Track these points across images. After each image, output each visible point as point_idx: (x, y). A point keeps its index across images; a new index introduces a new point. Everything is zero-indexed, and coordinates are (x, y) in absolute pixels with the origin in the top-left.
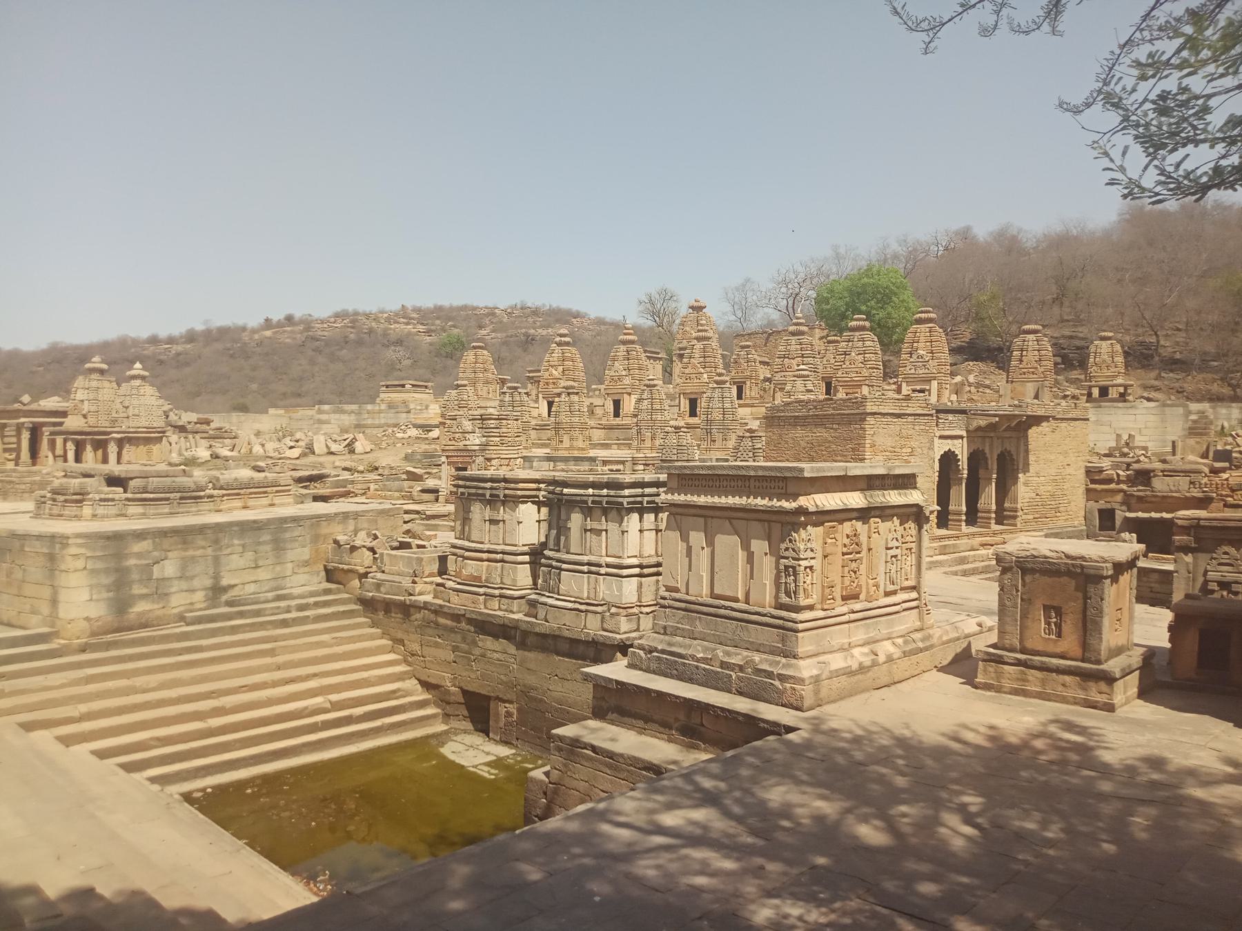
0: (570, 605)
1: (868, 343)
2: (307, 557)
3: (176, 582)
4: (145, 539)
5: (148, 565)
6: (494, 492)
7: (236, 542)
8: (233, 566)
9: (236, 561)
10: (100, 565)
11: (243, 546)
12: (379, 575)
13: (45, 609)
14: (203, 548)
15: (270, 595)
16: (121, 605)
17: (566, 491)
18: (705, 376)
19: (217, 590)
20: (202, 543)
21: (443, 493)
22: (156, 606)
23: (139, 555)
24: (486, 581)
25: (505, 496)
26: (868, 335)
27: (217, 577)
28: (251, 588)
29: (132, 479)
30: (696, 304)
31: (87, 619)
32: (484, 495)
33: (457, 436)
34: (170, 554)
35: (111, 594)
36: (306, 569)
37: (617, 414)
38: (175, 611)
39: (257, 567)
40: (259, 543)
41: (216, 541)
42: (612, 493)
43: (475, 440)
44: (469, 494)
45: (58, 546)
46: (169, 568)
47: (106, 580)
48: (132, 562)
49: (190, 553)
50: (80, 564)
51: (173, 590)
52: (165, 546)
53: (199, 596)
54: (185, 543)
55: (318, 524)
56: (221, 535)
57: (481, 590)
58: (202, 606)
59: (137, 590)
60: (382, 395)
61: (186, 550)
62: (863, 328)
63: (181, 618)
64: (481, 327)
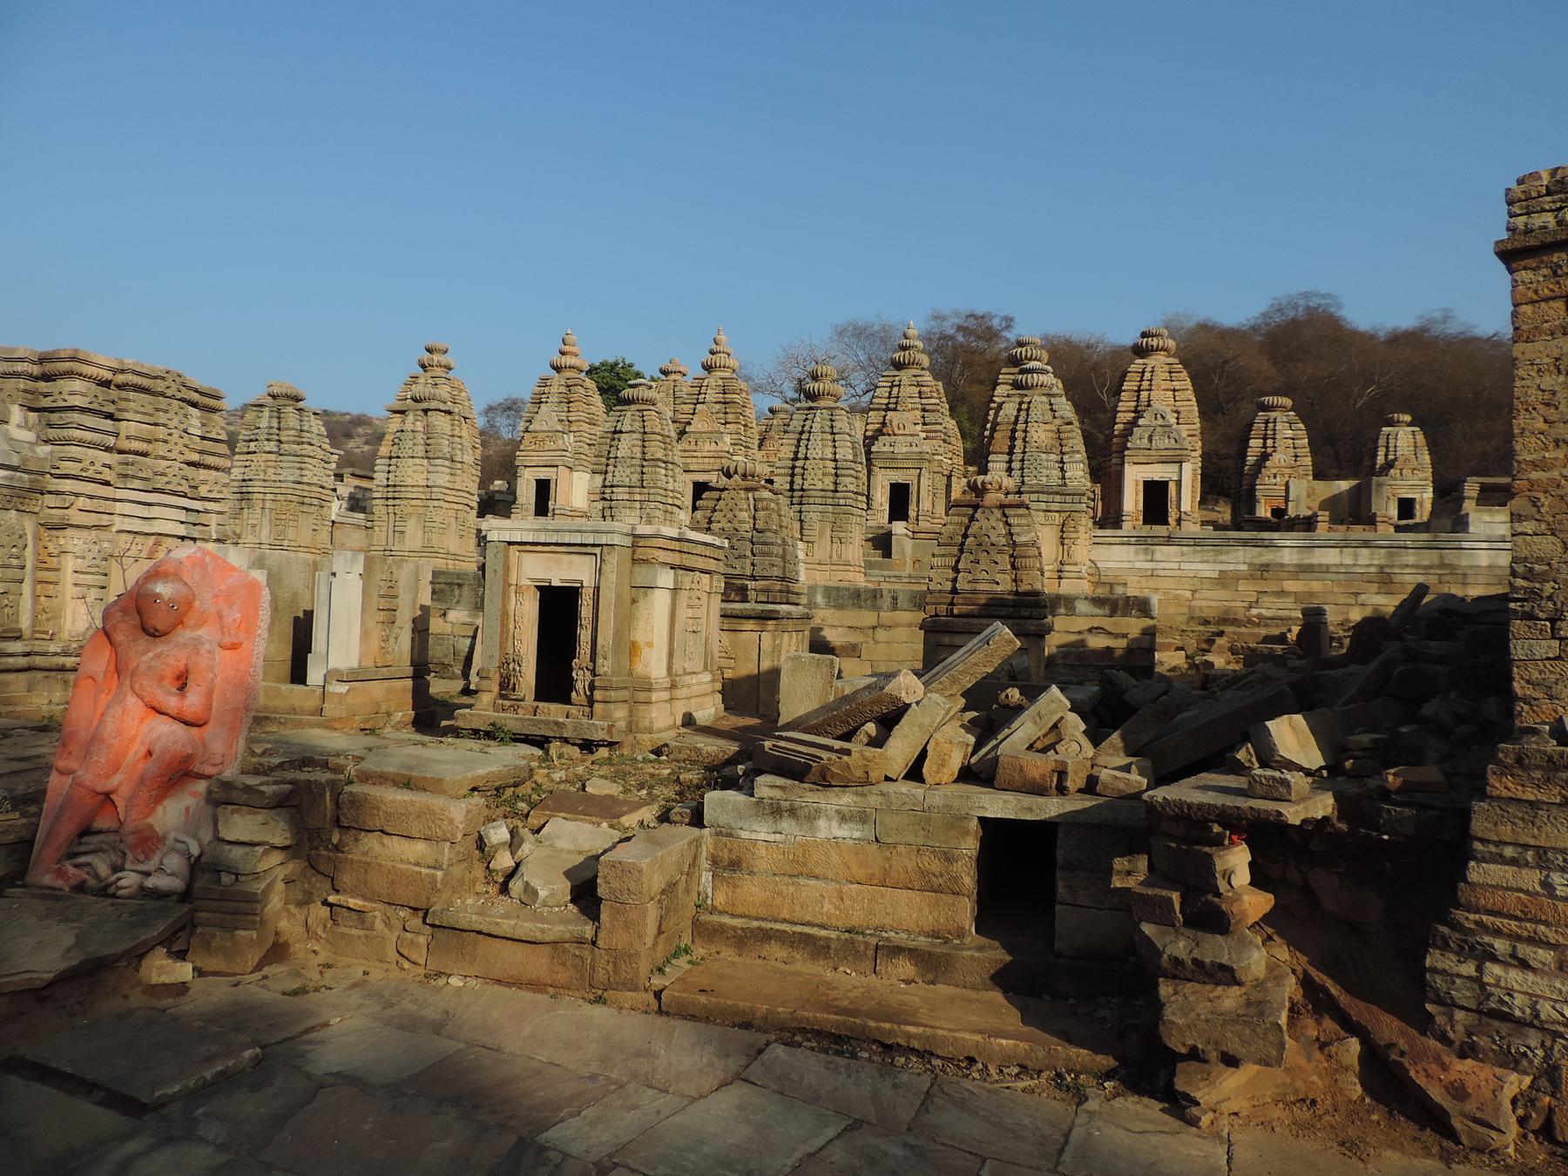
18: (727, 439)
37: (542, 508)
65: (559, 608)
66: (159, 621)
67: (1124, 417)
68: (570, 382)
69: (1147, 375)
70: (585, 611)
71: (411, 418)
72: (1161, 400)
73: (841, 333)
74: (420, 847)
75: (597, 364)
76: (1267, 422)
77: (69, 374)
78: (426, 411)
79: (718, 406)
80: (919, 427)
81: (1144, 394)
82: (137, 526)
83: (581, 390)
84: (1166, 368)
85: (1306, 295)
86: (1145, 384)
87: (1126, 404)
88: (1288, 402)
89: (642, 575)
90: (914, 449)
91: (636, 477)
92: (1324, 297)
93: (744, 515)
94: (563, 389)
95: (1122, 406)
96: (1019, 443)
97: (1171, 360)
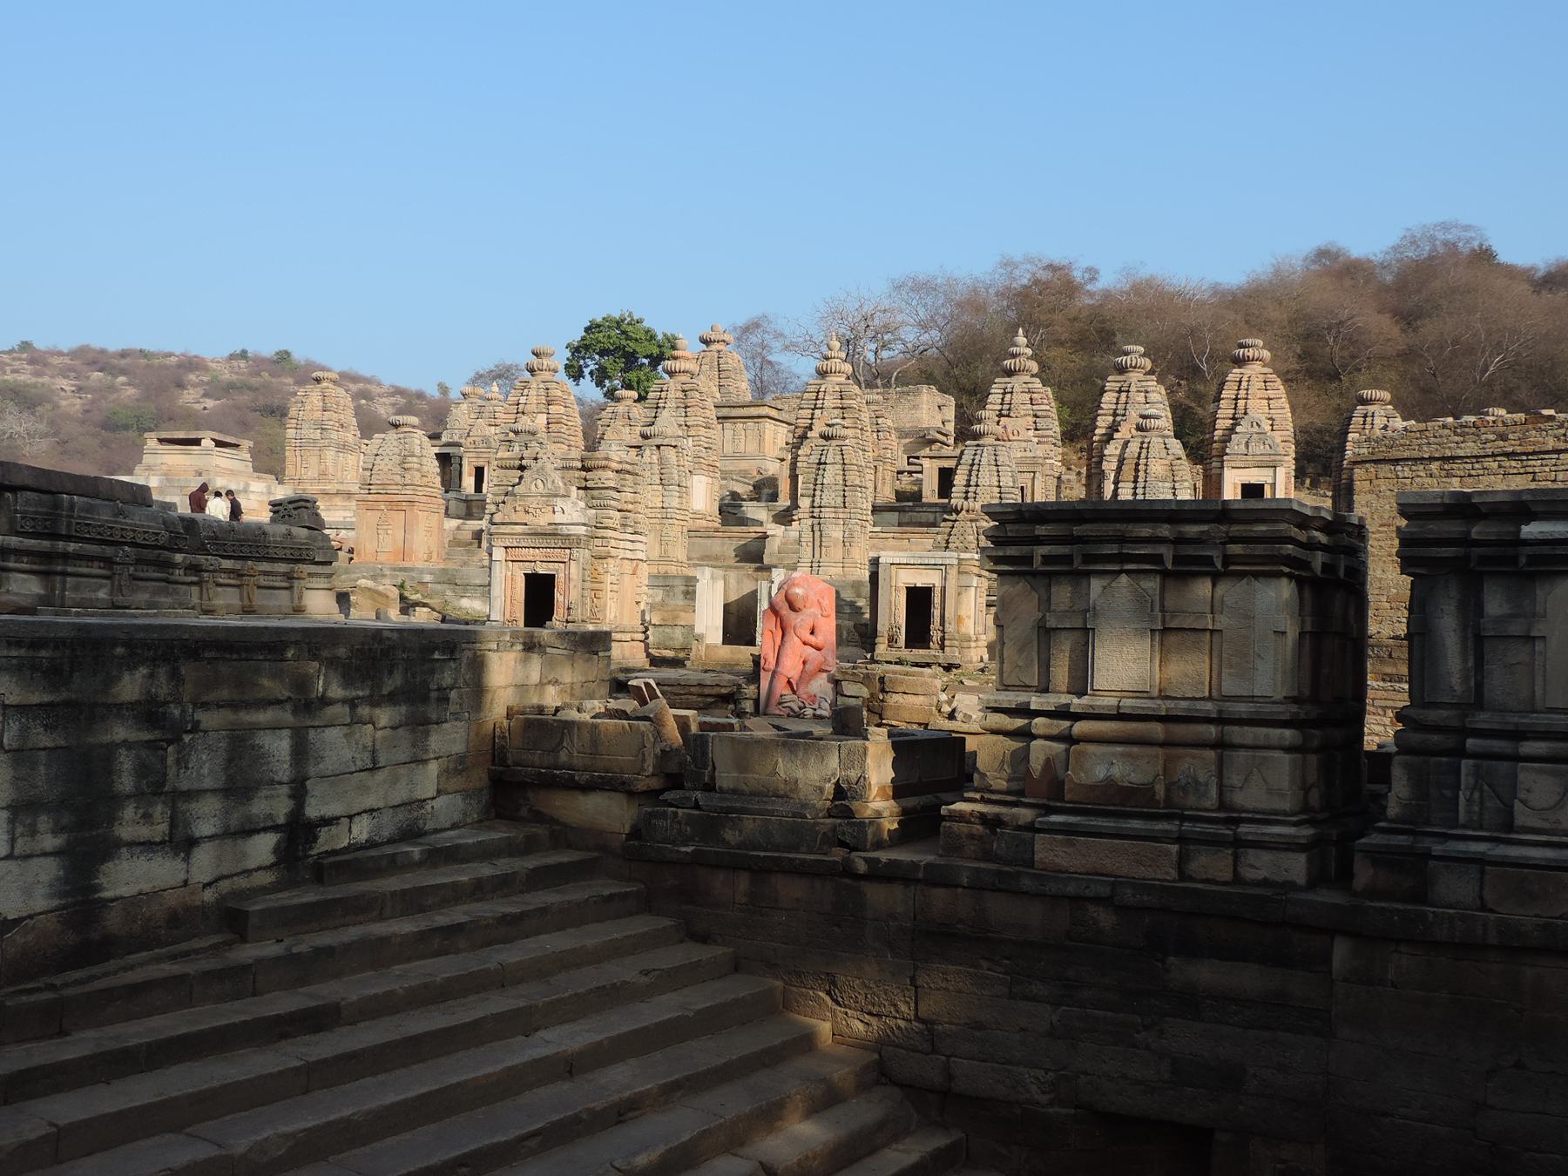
2: (459, 748)
5: (149, 745)
6: (1190, 551)
8: (330, 763)
9: (336, 745)
11: (352, 703)
17: (1531, 530)
24: (1168, 801)
25: (1227, 560)
26: (1152, 383)
27: (299, 791)
28: (361, 830)
39: (374, 768)
43: (571, 512)
53: (263, 848)
58: (266, 878)
59: (129, 825)
60: (147, 459)
64: (181, 385)
65: (919, 600)
66: (798, 605)
67: (1223, 424)
68: (686, 387)
69: (1244, 384)
70: (937, 600)
71: (648, 452)
72: (1257, 409)
73: (898, 288)
74: (921, 698)
75: (599, 320)
76: (1365, 416)
77: (604, 468)
78: (658, 447)
79: (837, 412)
80: (1031, 433)
81: (1241, 403)
82: (629, 555)
83: (697, 395)
84: (1262, 378)
85: (1445, 227)
86: (1242, 393)
87: (1225, 411)
88: (1387, 395)
89: (964, 580)
90: (1029, 454)
91: (839, 500)
92: (1467, 228)
93: (971, 538)
94: (681, 395)
95: (1220, 414)
96: (1141, 474)
97: (1266, 370)
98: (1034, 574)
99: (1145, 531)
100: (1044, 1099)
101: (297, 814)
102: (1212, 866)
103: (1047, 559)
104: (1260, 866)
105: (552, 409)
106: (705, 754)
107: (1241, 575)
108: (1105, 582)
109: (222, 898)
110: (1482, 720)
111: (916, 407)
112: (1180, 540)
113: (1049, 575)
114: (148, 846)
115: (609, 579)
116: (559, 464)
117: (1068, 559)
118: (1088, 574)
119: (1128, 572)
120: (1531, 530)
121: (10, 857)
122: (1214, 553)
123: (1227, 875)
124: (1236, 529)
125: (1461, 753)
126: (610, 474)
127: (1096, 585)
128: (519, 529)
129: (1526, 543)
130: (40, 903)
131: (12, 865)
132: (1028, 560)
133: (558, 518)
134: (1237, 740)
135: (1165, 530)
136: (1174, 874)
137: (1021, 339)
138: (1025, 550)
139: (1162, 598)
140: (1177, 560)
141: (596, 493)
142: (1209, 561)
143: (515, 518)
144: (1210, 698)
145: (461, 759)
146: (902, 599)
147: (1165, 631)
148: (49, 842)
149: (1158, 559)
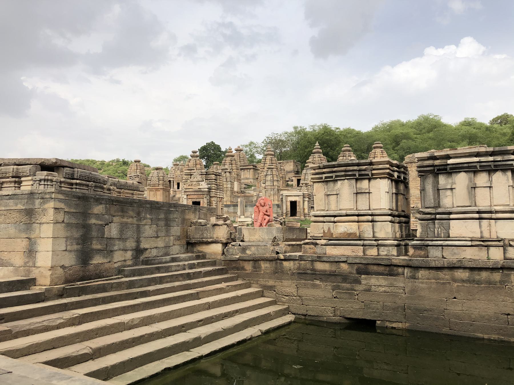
0: (469, 243)
1: (353, 158)
2: (179, 234)
3: (117, 242)
4: (101, 204)
5: (101, 225)
6: (363, 173)
7: (148, 216)
10: (73, 221)
11: (151, 219)
12: (241, 243)
13: (18, 260)
14: (132, 217)
15: (168, 258)
16: (85, 256)
17: (450, 161)
19: (139, 251)
20: (131, 213)
21: (294, 185)
22: (105, 261)
23: (98, 216)
25: (372, 175)
26: (352, 154)
27: (138, 242)
28: (154, 252)
29: (64, 167)
30: (239, 149)
31: (63, 267)
32: (355, 175)
33: (194, 183)
34: (114, 218)
35: (79, 247)
36: (178, 242)
38: (116, 265)
39: (157, 237)
40: (159, 220)
41: (139, 214)
42: (499, 158)
43: (204, 186)
44: (336, 176)
45: (37, 202)
46: (113, 231)
47: (77, 234)
48: (93, 221)
49: (125, 220)
50: (60, 217)
51: (116, 248)
52: (112, 212)
53: (129, 255)
54: (122, 211)
55: (183, 212)
56: (141, 209)
57: (361, 242)
58: (129, 263)
61: (123, 217)
62: (349, 151)
63: (120, 272)
65: (294, 205)
98: (323, 182)
99: (351, 168)
100: (331, 315)
101: (138, 246)
102: (373, 252)
103: (326, 177)
104: (383, 252)
105: (197, 166)
106: (241, 232)
107: (376, 178)
108: (341, 182)
109: (119, 267)
110: (440, 210)
111: (290, 165)
112: (359, 170)
113: (327, 181)
114: (99, 251)
115: (214, 202)
116: (200, 173)
117: (332, 177)
118: (337, 180)
119: (347, 179)
120: (450, 161)
121: (66, 250)
122: (370, 173)
123: (376, 254)
124: (374, 167)
125: (435, 219)
126: (214, 176)
127: (339, 183)
128: (191, 190)
129: (449, 165)
130: (73, 263)
131: (67, 253)
132: (322, 178)
133: (201, 187)
134: (377, 220)
135: (356, 168)
136: (362, 254)
137: (317, 144)
138: (320, 176)
139: (356, 185)
140: (359, 175)
141: (211, 181)
142: (368, 175)
143: (190, 187)
144: (370, 210)
145: (179, 237)
146: (289, 204)
147: (357, 193)
148: (75, 247)
149: (355, 175)
